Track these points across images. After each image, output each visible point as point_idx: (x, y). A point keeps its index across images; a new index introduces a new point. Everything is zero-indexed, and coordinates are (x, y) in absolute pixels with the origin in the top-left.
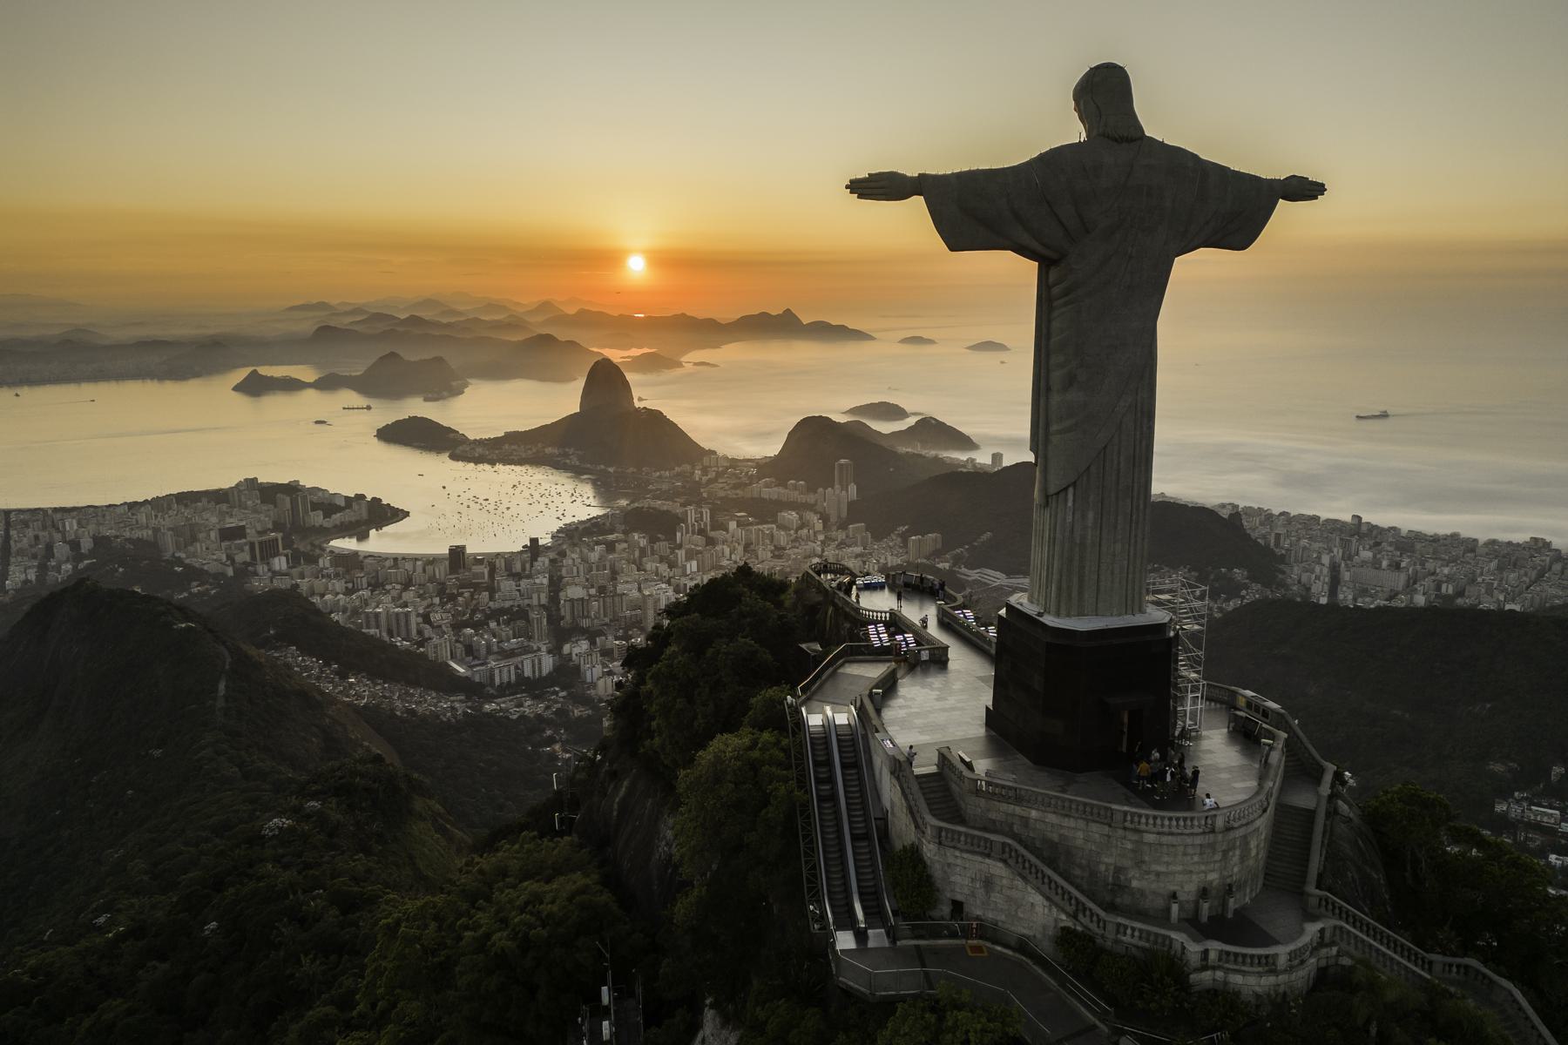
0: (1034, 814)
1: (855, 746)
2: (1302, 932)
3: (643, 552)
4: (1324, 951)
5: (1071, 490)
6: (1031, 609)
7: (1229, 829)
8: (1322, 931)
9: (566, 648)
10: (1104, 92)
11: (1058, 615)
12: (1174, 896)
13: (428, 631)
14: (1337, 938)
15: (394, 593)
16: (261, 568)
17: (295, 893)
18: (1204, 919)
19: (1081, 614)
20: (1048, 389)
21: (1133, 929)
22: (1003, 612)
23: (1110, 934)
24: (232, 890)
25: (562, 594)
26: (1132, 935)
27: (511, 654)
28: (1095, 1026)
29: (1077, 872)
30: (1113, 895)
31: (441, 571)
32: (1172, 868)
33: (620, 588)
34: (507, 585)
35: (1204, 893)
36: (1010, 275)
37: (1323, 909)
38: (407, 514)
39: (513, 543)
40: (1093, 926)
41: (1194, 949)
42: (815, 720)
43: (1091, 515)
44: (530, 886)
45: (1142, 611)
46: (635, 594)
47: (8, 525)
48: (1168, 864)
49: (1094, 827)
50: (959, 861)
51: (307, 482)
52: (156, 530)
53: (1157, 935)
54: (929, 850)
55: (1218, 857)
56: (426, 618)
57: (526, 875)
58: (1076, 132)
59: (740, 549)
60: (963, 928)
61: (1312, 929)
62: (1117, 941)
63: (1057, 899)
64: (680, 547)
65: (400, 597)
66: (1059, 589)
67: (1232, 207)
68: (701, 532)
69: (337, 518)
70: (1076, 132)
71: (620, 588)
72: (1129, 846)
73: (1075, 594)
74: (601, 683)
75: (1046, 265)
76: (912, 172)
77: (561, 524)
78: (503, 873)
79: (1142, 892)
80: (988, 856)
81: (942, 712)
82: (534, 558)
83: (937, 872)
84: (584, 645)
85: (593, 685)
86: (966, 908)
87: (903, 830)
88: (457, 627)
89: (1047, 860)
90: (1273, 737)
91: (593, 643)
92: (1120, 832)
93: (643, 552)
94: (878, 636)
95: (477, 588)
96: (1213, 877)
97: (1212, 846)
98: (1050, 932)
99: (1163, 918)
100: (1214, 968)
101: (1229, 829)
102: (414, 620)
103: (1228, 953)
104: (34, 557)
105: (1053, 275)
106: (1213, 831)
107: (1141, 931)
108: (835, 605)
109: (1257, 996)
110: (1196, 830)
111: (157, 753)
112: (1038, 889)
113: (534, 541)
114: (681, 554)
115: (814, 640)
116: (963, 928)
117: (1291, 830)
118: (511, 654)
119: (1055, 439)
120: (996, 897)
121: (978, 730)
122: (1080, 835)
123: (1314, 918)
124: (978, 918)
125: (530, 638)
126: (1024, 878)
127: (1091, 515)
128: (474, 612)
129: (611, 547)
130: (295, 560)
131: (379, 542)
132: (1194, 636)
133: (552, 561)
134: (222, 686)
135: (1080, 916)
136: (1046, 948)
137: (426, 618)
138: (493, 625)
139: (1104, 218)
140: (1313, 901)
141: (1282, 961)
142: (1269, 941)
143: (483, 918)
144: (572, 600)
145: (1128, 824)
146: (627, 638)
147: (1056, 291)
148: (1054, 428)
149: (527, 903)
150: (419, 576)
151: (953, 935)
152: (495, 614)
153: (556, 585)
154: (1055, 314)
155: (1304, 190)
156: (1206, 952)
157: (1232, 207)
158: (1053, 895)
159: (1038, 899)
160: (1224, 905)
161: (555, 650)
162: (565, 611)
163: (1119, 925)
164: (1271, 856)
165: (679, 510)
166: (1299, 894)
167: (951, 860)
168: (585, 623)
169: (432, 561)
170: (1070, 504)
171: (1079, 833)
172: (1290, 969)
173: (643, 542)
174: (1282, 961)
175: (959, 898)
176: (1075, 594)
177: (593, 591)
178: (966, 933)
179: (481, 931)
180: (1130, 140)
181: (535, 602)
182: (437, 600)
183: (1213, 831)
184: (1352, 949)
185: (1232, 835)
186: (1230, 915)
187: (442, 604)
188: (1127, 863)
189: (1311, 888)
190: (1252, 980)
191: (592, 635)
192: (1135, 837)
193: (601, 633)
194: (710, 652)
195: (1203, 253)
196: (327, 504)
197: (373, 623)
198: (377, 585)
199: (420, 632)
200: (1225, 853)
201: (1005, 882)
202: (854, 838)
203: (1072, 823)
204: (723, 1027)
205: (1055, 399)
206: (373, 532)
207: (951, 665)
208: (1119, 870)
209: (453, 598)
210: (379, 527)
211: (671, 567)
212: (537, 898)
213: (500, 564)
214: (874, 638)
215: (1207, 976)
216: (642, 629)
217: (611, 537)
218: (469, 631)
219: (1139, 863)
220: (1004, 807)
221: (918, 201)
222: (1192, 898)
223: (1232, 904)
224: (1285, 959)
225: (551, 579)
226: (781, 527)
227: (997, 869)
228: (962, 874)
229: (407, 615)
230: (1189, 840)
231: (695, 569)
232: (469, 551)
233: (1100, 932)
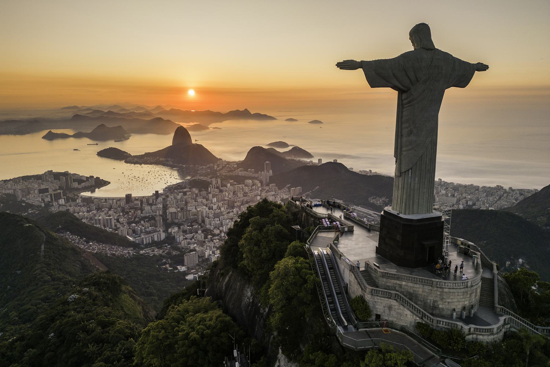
0: (404, 283)
2: (498, 320)
3: (197, 195)
4: (506, 326)
5: (410, 171)
6: (395, 212)
7: (472, 286)
8: (505, 320)
9: (170, 230)
11: (405, 214)
12: (454, 310)
13: (118, 225)
14: (509, 322)
15: (106, 212)
16: (55, 204)
17: (84, 322)
18: (464, 317)
19: (413, 213)
20: (402, 135)
21: (443, 322)
22: (382, 213)
23: (435, 324)
24: (58, 322)
25: (167, 211)
26: (443, 324)
27: (149, 233)
28: (434, 356)
29: (419, 303)
30: (433, 310)
31: (123, 203)
32: (453, 300)
33: (189, 208)
34: (147, 208)
35: (464, 308)
37: (501, 312)
38: (109, 183)
39: (149, 193)
40: (428, 321)
41: (466, 328)
42: (316, 253)
43: (417, 179)
44: (200, 315)
45: (432, 212)
46: (194, 210)
48: (452, 299)
49: (426, 287)
50: (379, 301)
51: (72, 171)
52: (14, 190)
53: (452, 324)
54: (368, 297)
55: (468, 296)
56: (118, 220)
57: (196, 312)
59: (232, 193)
60: (380, 324)
61: (502, 319)
62: (437, 326)
63: (415, 312)
64: (210, 193)
65: (108, 213)
66: (406, 205)
67: (461, 73)
68: (218, 188)
69: (83, 184)
70: (411, 48)
71: (189, 208)
72: (439, 293)
73: (411, 207)
75: (401, 92)
76: (359, 60)
77: (166, 186)
78: (187, 311)
79: (443, 309)
80: (390, 298)
81: (359, 248)
82: (157, 198)
83: (371, 305)
84: (176, 229)
85: (180, 243)
86: (381, 317)
87: (355, 290)
88: (129, 223)
89: (409, 299)
90: (476, 254)
91: (179, 228)
92: (435, 289)
93: (197, 195)
94: (326, 223)
95: (136, 209)
96: (467, 303)
97: (467, 292)
98: (413, 324)
99: (451, 317)
100: (473, 334)
101: (472, 286)
102: (113, 222)
103: (477, 329)
105: (404, 96)
106: (467, 287)
107: (446, 322)
108: (306, 212)
109: (487, 342)
110: (462, 287)
111: (19, 272)
112: (408, 309)
113: (157, 192)
114: (210, 195)
115: (297, 224)
116: (380, 324)
117: (488, 285)
118: (149, 233)
119: (404, 153)
120: (393, 313)
121: (373, 255)
122: (421, 290)
123: (502, 316)
124: (386, 320)
125: (156, 227)
126: (403, 306)
127: (417, 179)
128: (135, 218)
129: (185, 194)
130: (67, 200)
131: (99, 193)
132: (447, 221)
133: (164, 199)
134: (43, 247)
135: (424, 318)
136: (411, 330)
137: (118, 220)
138: (142, 222)
139: (420, 77)
140: (498, 310)
141: (495, 331)
142: (489, 325)
143: (184, 327)
144: (171, 213)
145: (438, 286)
146: (192, 226)
147: (405, 102)
148: (404, 149)
149: (200, 321)
150: (114, 205)
151: (377, 326)
152: (143, 218)
153: (165, 208)
154: (405, 110)
155: (482, 67)
156: (470, 329)
157: (461, 73)
158: (414, 310)
159: (408, 313)
160: (470, 312)
161: (166, 231)
162: (169, 217)
163: (438, 321)
164: (481, 295)
165: (209, 180)
166: (492, 307)
167: (376, 300)
168: (176, 221)
169: (119, 200)
170: (410, 175)
171: (420, 289)
172: (497, 333)
173: (197, 192)
174: (495, 331)
175: (379, 313)
176: (411, 207)
177: (179, 209)
178: (382, 325)
179: (185, 332)
180: (431, 50)
181: (158, 214)
182: (121, 214)
183: (467, 287)
184: (514, 325)
185: (473, 288)
186: (472, 316)
187: (123, 215)
188: (438, 299)
189: (497, 305)
190: (486, 337)
191: (179, 225)
192: (441, 290)
193: (182, 224)
194: (265, 230)
195: (452, 88)
196: (79, 180)
197: (98, 222)
198: (99, 209)
199: (115, 226)
200: (471, 294)
201: (396, 307)
202: (337, 294)
203: (418, 286)
204: (289, 362)
205: (404, 139)
206: (97, 190)
207: (354, 232)
208: (435, 302)
209: (127, 213)
210: (99, 188)
211: (207, 200)
212: (203, 320)
213: (144, 200)
214: (324, 223)
215: (470, 337)
216: (197, 223)
217: (185, 190)
218: (134, 225)
219: (442, 299)
220: (393, 281)
221: (361, 70)
222: (460, 310)
223: (473, 312)
224: (493, 330)
225: (163, 205)
226: (246, 185)
227: (394, 303)
228: (380, 305)
229: (111, 219)
230: (459, 291)
231: (215, 201)
233: (431, 323)
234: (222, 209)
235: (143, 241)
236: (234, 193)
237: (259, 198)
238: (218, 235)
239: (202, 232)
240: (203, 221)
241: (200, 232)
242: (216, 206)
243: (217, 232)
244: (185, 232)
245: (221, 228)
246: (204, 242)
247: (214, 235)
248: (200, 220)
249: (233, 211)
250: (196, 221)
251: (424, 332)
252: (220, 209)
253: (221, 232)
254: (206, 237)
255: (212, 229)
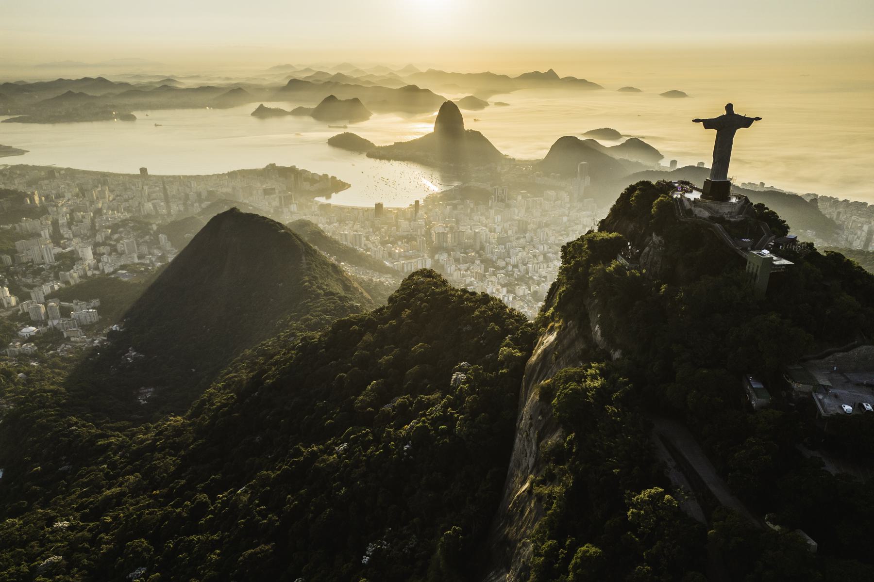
1: (681, 200)
9: (437, 257)
10: (729, 107)
15: (350, 225)
27: (410, 258)
30: (717, 212)
36: (714, 132)
39: (405, 204)
47: (164, 183)
51: (300, 167)
52: (234, 188)
56: (367, 239)
58: (725, 113)
67: (746, 122)
71: (462, 228)
74: (455, 273)
85: (452, 275)
88: (383, 243)
89: (708, 208)
91: (449, 255)
102: (364, 239)
104: (180, 199)
113: (417, 202)
131: (337, 199)
138: (400, 243)
146: (467, 253)
152: (401, 238)
155: (758, 119)
157: (746, 122)
161: (432, 257)
165: (490, 189)
168: (445, 245)
182: (371, 230)
187: (374, 232)
191: (448, 251)
193: (453, 250)
198: (341, 221)
209: (379, 229)
216: (474, 250)
217: (455, 202)
229: (360, 235)
232: (384, 206)
234: (510, 232)
235: (403, 268)
236: (528, 209)
237: (565, 219)
238: (503, 268)
239: (482, 262)
240: (482, 248)
241: (478, 262)
242: (500, 227)
243: (501, 263)
244: (457, 260)
245: (508, 260)
246: (485, 276)
247: (498, 268)
248: (478, 248)
249: (525, 237)
250: (471, 247)
251: (711, 218)
252: (506, 232)
253: (507, 264)
254: (486, 270)
255: (494, 259)
